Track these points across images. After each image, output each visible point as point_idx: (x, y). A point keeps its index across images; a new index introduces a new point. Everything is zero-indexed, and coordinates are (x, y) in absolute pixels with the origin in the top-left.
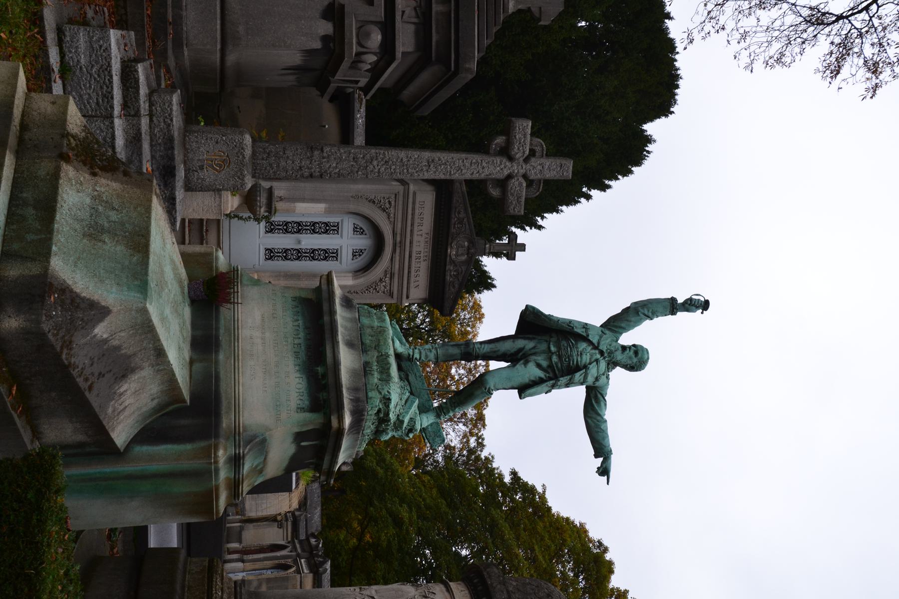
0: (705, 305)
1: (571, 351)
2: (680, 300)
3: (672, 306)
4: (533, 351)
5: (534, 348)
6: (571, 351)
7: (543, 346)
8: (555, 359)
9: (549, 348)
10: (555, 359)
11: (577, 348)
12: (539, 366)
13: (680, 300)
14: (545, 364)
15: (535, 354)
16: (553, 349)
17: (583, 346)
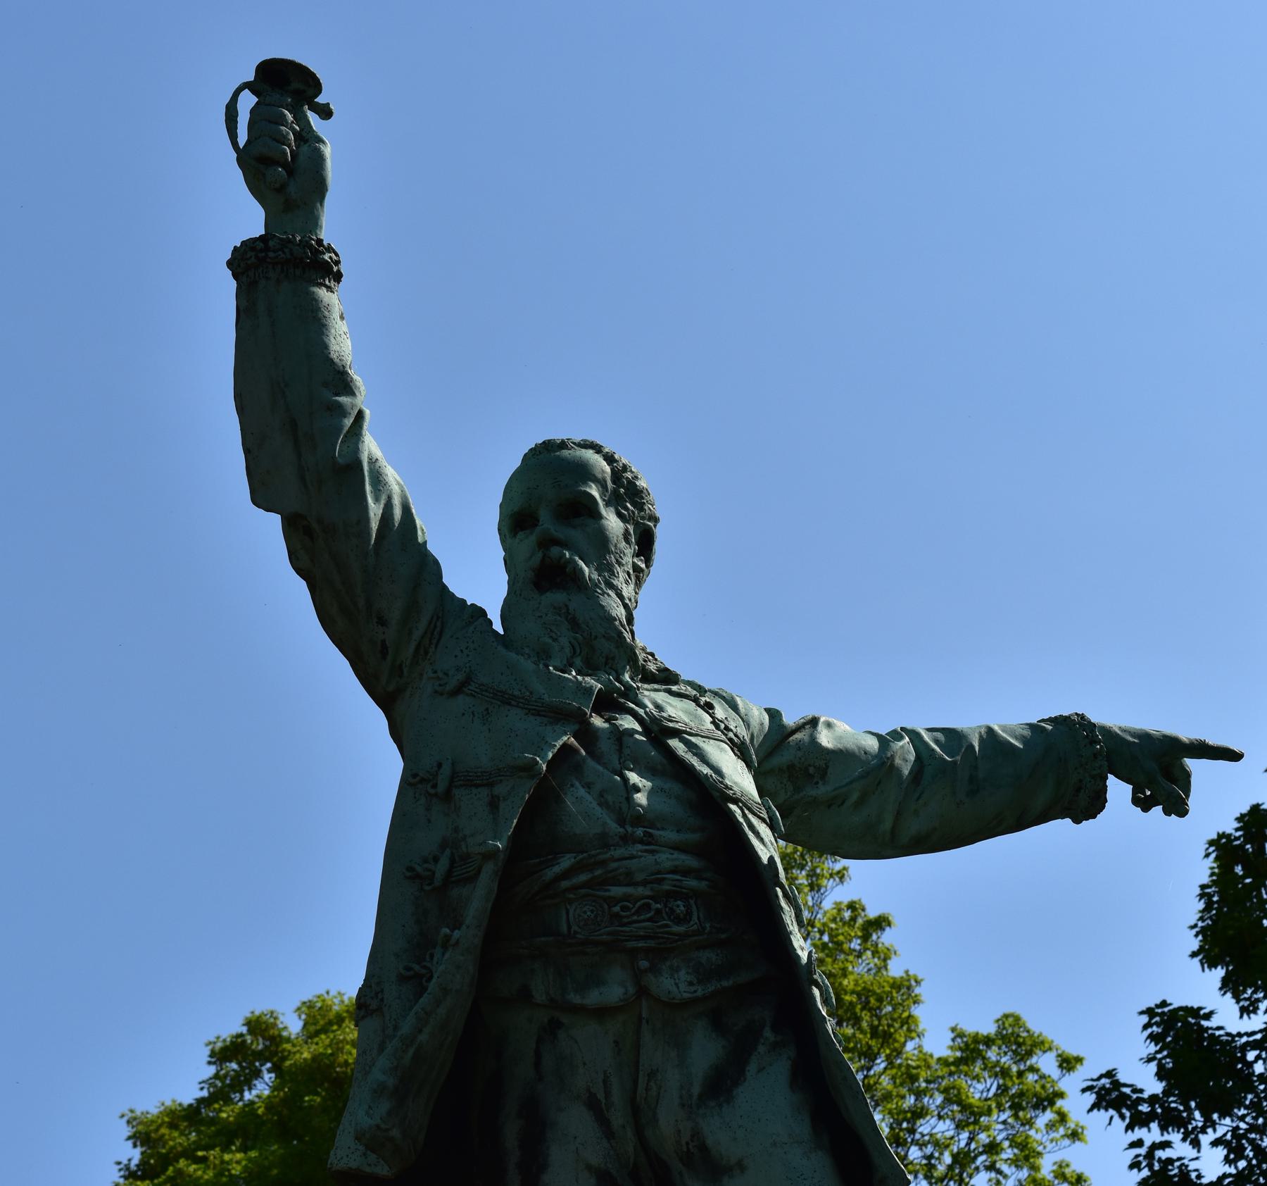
0: (285, 85)
1: (628, 879)
2: (249, 219)
3: (282, 276)
4: (618, 1118)
5: (594, 1106)
6: (628, 879)
7: (591, 1051)
8: (674, 983)
9: (601, 1013)
10: (674, 983)
11: (604, 841)
12: (721, 1085)
13: (249, 219)
14: (705, 1051)
15: (639, 1114)
16: (614, 990)
17: (580, 807)
